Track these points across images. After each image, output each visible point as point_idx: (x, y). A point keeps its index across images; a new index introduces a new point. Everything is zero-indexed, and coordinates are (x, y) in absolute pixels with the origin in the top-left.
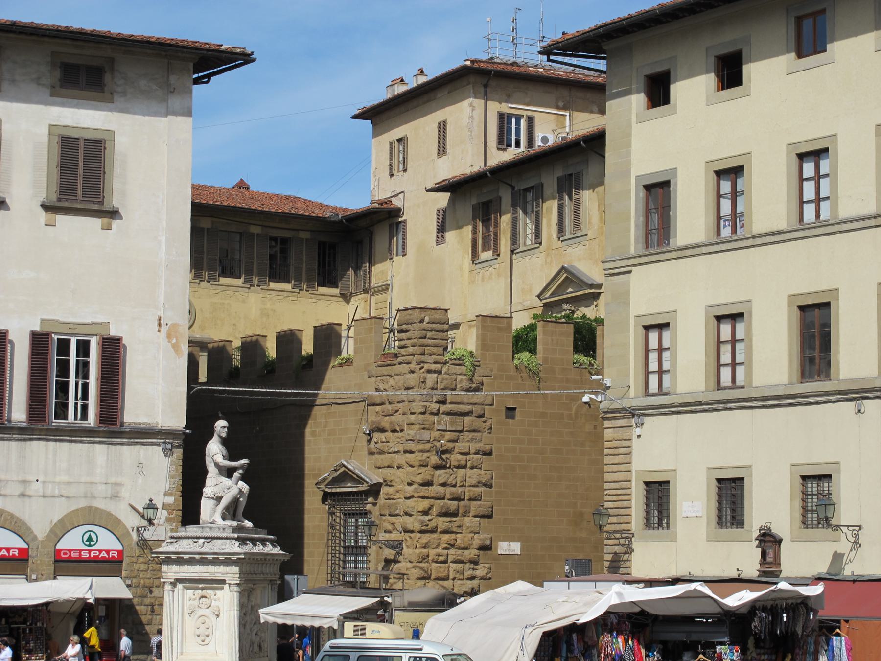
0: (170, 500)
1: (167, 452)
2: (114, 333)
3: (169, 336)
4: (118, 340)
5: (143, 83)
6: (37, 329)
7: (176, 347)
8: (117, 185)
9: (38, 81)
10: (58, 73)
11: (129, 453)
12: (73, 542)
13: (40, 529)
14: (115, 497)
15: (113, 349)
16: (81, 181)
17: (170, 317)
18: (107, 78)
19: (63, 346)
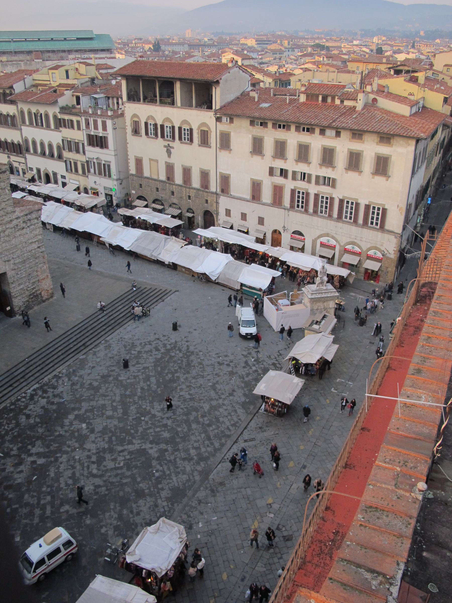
0: (395, 249)
1: (396, 237)
2: (386, 207)
3: (400, 210)
4: (386, 209)
5: (401, 142)
6: (367, 203)
7: (401, 213)
8: (391, 170)
9: (373, 141)
10: (379, 139)
11: (386, 236)
12: (371, 253)
13: (364, 249)
14: (382, 245)
15: (385, 211)
16: (382, 166)
17: (401, 205)
18: (392, 141)
19: (374, 208)
